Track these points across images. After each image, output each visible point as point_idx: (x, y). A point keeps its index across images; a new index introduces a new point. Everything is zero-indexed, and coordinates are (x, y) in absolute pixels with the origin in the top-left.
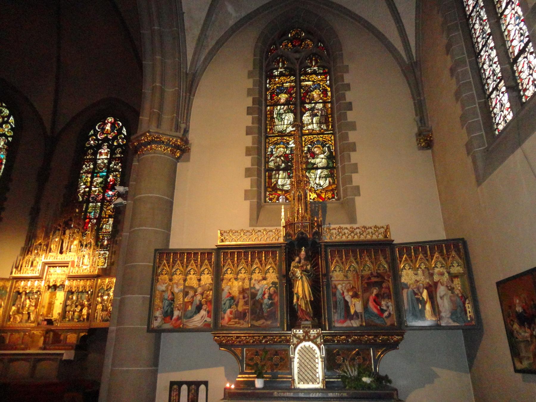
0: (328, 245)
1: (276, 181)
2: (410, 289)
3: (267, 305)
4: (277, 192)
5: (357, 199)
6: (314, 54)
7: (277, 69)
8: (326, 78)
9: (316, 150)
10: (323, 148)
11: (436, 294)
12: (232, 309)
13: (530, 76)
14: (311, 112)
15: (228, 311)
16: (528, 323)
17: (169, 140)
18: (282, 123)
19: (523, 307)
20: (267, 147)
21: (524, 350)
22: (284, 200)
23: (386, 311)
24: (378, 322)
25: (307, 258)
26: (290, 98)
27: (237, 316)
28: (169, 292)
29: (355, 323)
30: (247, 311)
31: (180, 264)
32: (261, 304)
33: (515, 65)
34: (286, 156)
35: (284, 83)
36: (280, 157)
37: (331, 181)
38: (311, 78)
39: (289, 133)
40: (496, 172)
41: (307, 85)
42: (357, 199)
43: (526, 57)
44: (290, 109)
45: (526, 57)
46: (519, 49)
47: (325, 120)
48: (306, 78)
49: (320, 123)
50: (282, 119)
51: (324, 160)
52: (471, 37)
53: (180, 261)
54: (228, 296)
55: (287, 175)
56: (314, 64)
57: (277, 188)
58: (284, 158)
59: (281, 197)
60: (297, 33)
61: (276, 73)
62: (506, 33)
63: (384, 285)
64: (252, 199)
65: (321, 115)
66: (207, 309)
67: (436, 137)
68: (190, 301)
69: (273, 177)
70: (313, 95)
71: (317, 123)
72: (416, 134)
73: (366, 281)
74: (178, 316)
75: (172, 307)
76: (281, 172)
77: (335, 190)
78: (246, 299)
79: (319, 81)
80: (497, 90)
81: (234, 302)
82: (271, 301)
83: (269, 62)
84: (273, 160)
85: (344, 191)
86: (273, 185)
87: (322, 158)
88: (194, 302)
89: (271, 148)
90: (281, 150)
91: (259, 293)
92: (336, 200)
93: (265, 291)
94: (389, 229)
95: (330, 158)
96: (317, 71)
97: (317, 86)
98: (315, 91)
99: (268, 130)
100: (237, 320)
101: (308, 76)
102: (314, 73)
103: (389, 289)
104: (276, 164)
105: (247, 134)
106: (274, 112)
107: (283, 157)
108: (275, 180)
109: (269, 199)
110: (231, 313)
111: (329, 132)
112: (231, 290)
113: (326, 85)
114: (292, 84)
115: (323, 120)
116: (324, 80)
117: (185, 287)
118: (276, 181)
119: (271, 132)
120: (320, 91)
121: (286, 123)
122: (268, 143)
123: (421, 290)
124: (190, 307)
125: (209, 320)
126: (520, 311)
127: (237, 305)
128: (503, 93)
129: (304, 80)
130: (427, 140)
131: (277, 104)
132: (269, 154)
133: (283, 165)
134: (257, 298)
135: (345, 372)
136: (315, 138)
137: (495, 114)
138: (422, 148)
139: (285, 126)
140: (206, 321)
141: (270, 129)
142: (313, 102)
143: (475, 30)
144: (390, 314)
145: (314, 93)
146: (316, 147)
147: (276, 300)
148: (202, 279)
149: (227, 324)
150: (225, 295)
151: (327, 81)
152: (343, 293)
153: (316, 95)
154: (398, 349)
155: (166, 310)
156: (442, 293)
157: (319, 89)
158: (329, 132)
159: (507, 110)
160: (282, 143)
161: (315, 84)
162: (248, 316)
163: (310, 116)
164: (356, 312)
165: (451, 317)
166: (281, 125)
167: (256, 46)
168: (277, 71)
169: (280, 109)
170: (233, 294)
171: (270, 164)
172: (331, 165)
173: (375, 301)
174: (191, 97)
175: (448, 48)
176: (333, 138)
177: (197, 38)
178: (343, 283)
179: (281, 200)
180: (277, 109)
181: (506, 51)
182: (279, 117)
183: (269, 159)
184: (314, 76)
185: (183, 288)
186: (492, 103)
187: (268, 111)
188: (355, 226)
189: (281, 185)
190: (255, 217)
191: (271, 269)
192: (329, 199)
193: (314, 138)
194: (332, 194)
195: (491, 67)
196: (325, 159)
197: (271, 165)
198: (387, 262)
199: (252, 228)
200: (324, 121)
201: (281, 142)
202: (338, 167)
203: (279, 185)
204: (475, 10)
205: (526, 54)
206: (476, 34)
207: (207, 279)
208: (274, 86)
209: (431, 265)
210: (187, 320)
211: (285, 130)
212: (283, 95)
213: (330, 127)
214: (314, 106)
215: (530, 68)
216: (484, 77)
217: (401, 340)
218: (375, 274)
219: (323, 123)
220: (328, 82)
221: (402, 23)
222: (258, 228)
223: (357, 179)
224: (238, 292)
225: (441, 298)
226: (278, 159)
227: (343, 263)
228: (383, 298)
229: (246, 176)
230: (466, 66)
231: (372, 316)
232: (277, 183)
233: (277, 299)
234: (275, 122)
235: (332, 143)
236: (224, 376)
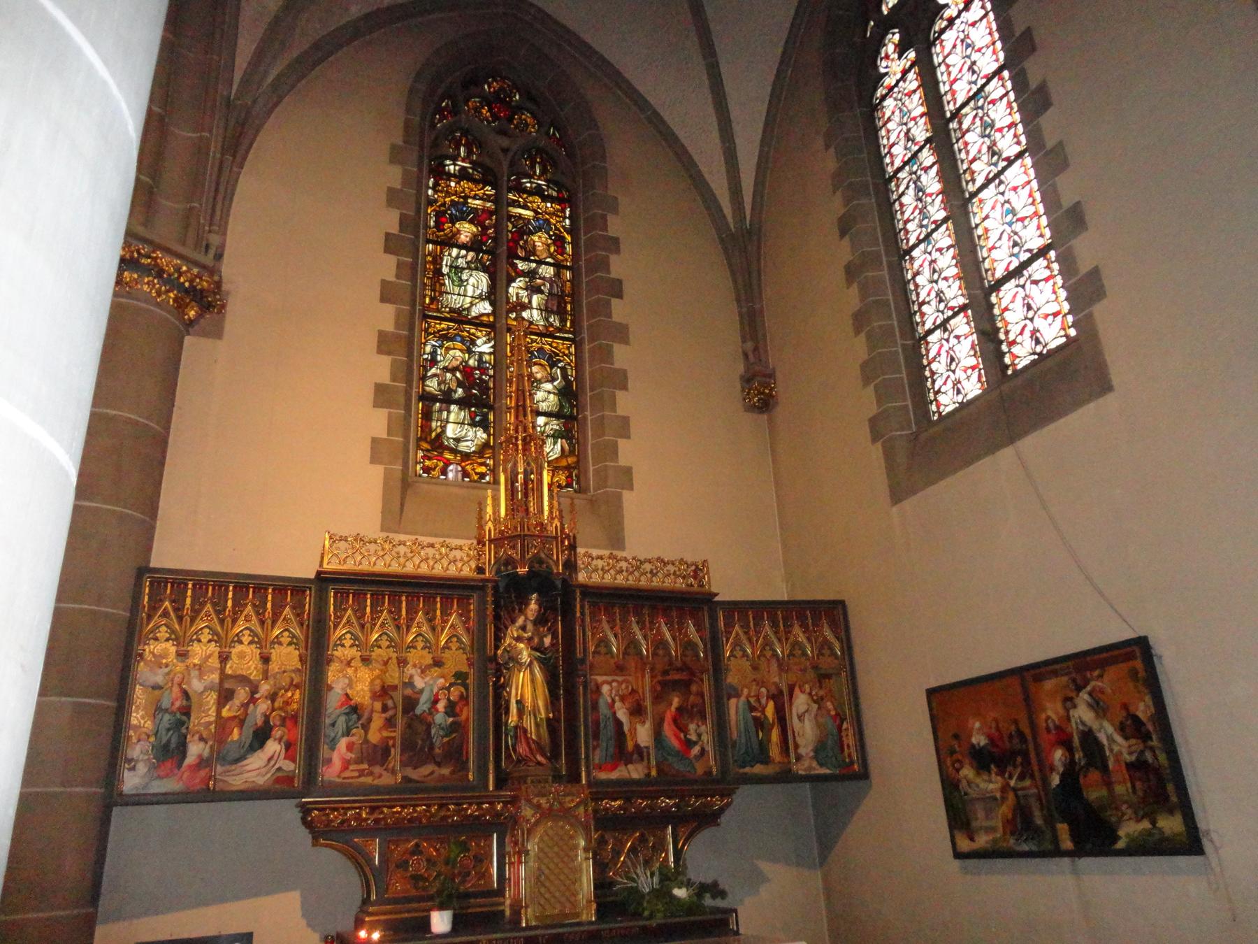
0: (588, 591)
1: (441, 427)
2: (743, 699)
3: (443, 729)
4: (442, 453)
5: (627, 495)
6: (540, 151)
7: (454, 159)
8: (563, 211)
9: (535, 369)
10: (551, 369)
11: (791, 710)
12: (354, 739)
13: (1028, 322)
14: (527, 280)
15: (343, 743)
16: (998, 766)
17: (178, 269)
18: (462, 292)
19: (990, 737)
20: (423, 341)
21: (981, 814)
22: (460, 475)
23: (695, 743)
24: (680, 767)
25: (540, 621)
27: (365, 755)
28: (176, 689)
29: (635, 772)
30: (391, 743)
31: (214, 616)
32: (429, 726)
33: (994, 294)
34: (467, 370)
35: (470, 197)
36: (453, 370)
37: (567, 447)
38: (530, 202)
39: (476, 318)
40: (943, 483)
41: (520, 217)
42: (627, 495)
43: (1023, 287)
44: (480, 261)
45: (1023, 287)
46: (1007, 269)
47: (555, 305)
48: (520, 200)
49: (546, 310)
50: (460, 280)
51: (552, 396)
52: (892, 217)
53: (214, 605)
54: (342, 705)
55: (468, 417)
56: (538, 171)
57: (442, 443)
58: (463, 376)
59: (451, 467)
60: (502, 89)
61: (452, 168)
62: (980, 231)
63: (694, 688)
64: (391, 463)
65: (550, 294)
66: (285, 738)
67: (783, 389)
68: (235, 717)
69: (435, 416)
70: (534, 242)
71: (541, 310)
72: (742, 377)
73: (660, 678)
74: (200, 756)
75: (184, 730)
76: (454, 407)
77: (574, 468)
78: (390, 713)
80: (945, 330)
81: (359, 719)
82: (451, 719)
83: (436, 138)
84: (435, 375)
85: (597, 472)
86: (434, 435)
87: (549, 392)
88: (249, 718)
89: (433, 346)
90: (455, 355)
91: (424, 698)
92: (575, 491)
93: (437, 694)
94: (708, 568)
95: (566, 393)
96: (544, 190)
97: (544, 226)
98: (539, 234)
99: (427, 300)
100: (365, 766)
101: (525, 196)
102: (538, 191)
103: (702, 695)
104: (443, 387)
105: (384, 299)
106: (442, 259)
107: (461, 372)
108: (439, 424)
109: (422, 468)
110: (350, 747)
111: (566, 335)
112: (351, 688)
113: (563, 227)
114: (489, 205)
115: (553, 305)
117: (224, 677)
118: (441, 427)
119: (433, 306)
120: (550, 237)
121: (470, 293)
122: (426, 330)
123: (764, 701)
124: (236, 731)
125: (288, 766)
126: (982, 743)
127: (366, 727)
128: (958, 337)
129: (515, 204)
130: (763, 393)
131: (450, 242)
132: (426, 359)
133: (460, 391)
134: (418, 711)
135: (633, 880)
136: (536, 343)
137: (933, 373)
138: (752, 408)
139: (468, 300)
140: (279, 769)
141: (433, 300)
142: (532, 258)
143: (902, 205)
144: (703, 750)
145: (536, 238)
146: (535, 364)
147: (463, 717)
148: (273, 657)
149: (339, 776)
150: (333, 701)
151: (565, 218)
152: (614, 701)
153: (540, 244)
154: (718, 825)
155: (164, 740)
156: (802, 708)
157: (548, 234)
158: (566, 335)
159: (965, 371)
160: (459, 339)
161: (538, 219)
162: (395, 753)
163: (526, 289)
164: (637, 746)
165: (816, 758)
166: (459, 294)
167: (411, 91)
168: (455, 165)
169: (457, 257)
170: (357, 699)
171: (428, 382)
172: (567, 410)
173: (675, 720)
174: (235, 169)
175: (845, 227)
176: (573, 350)
177: (268, 19)
178: (613, 681)
179: (451, 475)
180: (450, 255)
181: (977, 263)
182: (456, 274)
183: (427, 371)
184: (538, 199)
185: (217, 681)
186: (928, 351)
187: (430, 254)
188: (620, 554)
189: (454, 439)
190: (397, 508)
191: (348, 636)
192: (560, 486)
193: (533, 341)
194: (567, 477)
195: (934, 284)
196: (554, 393)
197: (432, 385)
198: (468, 630)
199: (384, 535)
200: (555, 308)
201: (456, 335)
202: (585, 418)
203: (448, 438)
204: (907, 168)
205: (1022, 281)
206: (903, 213)
207: (287, 657)
208: (445, 197)
209: (438, 640)
210: (228, 767)
211: (468, 309)
212: (467, 225)
213: (568, 324)
214: (535, 269)
215: (1029, 308)
216: (914, 298)
217: (728, 805)
218: (679, 664)
219: (552, 312)
220: (567, 221)
221: (735, 143)
222: (402, 537)
223: (627, 452)
224: (368, 695)
225: (801, 717)
226: (449, 375)
227: (362, 626)
228: (692, 717)
229: (377, 404)
230: (883, 270)
231: (669, 754)
232: (443, 432)
233: (468, 713)
234: (444, 284)
235: (572, 361)
236: (299, 913)
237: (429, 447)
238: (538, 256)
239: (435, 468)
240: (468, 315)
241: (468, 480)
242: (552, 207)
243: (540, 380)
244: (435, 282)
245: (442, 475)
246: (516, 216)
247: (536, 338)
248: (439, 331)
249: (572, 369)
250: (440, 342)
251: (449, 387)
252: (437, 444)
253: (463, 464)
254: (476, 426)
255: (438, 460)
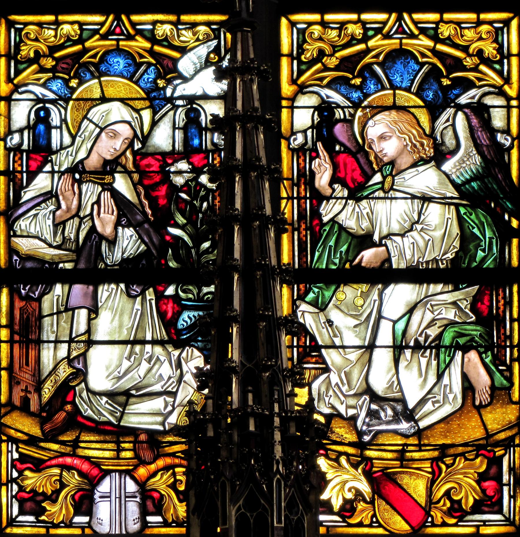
1: (70, 361)
4: (75, 444)
10: (434, 118)
59: (105, 486)
87: (426, 199)
89: (38, 100)
118: (70, 361)
183: (19, 189)
189: (111, 395)
196: (444, 201)
237: (36, 431)
239: (57, 492)
241: (159, 519)
243: (392, 163)
245: (77, 513)
247: (382, 17)
248: (53, 49)
249: (509, 107)
250: (56, 85)
251: (93, 229)
252: (61, 416)
253: (142, 471)
254: (180, 345)
255: (64, 467)
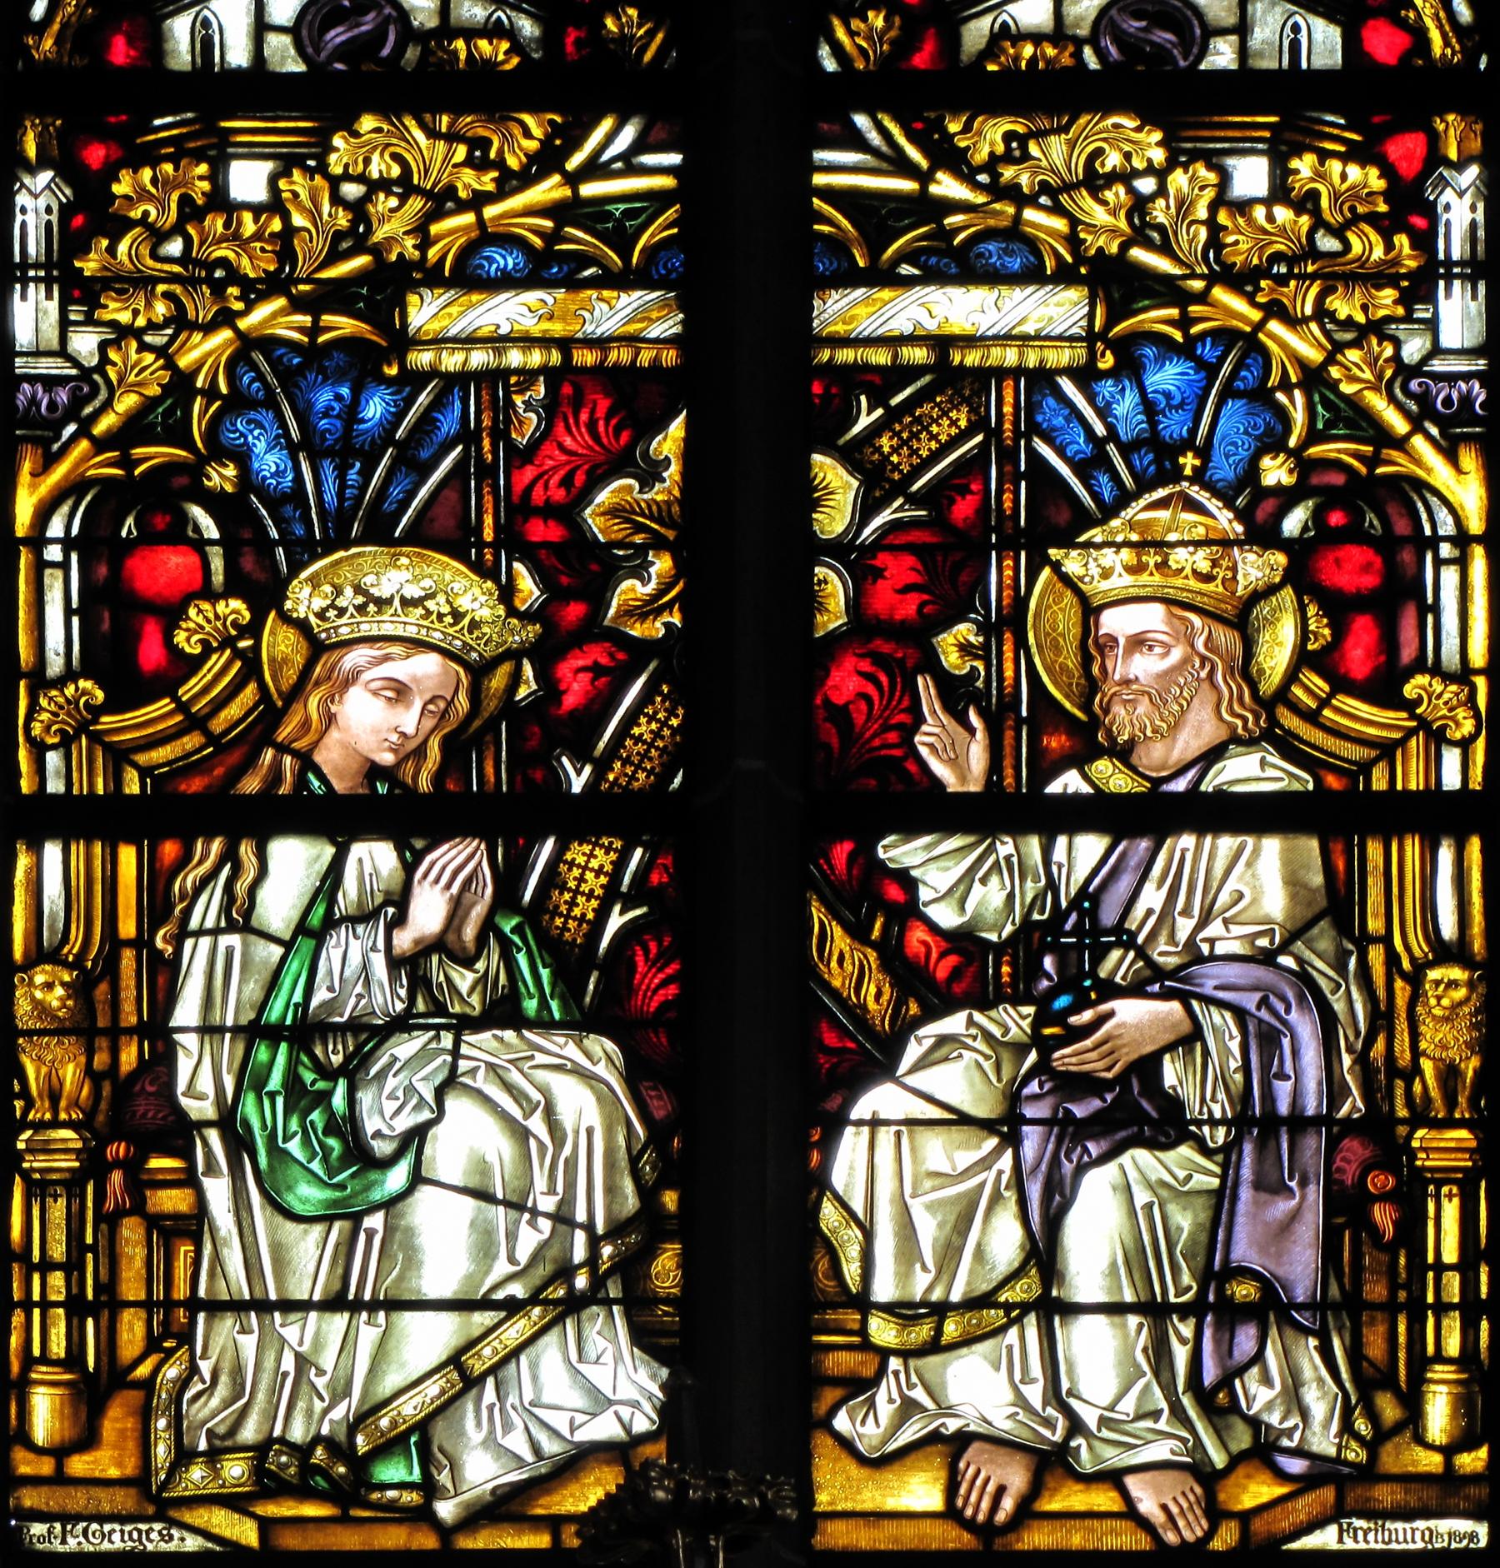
14: (1016, 1021)
26: (545, 654)
38: (1053, 194)
48: (947, 186)
71: (1155, 1311)
79: (1241, 280)
101: (992, 135)
116: (1367, 245)
142: (1069, 782)
182: (298, 1096)
234: (195, 1224)
238: (1123, 754)
240: (430, 1489)
242: (1280, 192)
244: (109, 1221)
246: (902, 374)
